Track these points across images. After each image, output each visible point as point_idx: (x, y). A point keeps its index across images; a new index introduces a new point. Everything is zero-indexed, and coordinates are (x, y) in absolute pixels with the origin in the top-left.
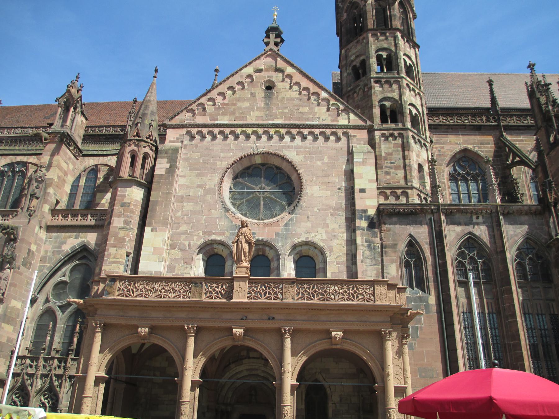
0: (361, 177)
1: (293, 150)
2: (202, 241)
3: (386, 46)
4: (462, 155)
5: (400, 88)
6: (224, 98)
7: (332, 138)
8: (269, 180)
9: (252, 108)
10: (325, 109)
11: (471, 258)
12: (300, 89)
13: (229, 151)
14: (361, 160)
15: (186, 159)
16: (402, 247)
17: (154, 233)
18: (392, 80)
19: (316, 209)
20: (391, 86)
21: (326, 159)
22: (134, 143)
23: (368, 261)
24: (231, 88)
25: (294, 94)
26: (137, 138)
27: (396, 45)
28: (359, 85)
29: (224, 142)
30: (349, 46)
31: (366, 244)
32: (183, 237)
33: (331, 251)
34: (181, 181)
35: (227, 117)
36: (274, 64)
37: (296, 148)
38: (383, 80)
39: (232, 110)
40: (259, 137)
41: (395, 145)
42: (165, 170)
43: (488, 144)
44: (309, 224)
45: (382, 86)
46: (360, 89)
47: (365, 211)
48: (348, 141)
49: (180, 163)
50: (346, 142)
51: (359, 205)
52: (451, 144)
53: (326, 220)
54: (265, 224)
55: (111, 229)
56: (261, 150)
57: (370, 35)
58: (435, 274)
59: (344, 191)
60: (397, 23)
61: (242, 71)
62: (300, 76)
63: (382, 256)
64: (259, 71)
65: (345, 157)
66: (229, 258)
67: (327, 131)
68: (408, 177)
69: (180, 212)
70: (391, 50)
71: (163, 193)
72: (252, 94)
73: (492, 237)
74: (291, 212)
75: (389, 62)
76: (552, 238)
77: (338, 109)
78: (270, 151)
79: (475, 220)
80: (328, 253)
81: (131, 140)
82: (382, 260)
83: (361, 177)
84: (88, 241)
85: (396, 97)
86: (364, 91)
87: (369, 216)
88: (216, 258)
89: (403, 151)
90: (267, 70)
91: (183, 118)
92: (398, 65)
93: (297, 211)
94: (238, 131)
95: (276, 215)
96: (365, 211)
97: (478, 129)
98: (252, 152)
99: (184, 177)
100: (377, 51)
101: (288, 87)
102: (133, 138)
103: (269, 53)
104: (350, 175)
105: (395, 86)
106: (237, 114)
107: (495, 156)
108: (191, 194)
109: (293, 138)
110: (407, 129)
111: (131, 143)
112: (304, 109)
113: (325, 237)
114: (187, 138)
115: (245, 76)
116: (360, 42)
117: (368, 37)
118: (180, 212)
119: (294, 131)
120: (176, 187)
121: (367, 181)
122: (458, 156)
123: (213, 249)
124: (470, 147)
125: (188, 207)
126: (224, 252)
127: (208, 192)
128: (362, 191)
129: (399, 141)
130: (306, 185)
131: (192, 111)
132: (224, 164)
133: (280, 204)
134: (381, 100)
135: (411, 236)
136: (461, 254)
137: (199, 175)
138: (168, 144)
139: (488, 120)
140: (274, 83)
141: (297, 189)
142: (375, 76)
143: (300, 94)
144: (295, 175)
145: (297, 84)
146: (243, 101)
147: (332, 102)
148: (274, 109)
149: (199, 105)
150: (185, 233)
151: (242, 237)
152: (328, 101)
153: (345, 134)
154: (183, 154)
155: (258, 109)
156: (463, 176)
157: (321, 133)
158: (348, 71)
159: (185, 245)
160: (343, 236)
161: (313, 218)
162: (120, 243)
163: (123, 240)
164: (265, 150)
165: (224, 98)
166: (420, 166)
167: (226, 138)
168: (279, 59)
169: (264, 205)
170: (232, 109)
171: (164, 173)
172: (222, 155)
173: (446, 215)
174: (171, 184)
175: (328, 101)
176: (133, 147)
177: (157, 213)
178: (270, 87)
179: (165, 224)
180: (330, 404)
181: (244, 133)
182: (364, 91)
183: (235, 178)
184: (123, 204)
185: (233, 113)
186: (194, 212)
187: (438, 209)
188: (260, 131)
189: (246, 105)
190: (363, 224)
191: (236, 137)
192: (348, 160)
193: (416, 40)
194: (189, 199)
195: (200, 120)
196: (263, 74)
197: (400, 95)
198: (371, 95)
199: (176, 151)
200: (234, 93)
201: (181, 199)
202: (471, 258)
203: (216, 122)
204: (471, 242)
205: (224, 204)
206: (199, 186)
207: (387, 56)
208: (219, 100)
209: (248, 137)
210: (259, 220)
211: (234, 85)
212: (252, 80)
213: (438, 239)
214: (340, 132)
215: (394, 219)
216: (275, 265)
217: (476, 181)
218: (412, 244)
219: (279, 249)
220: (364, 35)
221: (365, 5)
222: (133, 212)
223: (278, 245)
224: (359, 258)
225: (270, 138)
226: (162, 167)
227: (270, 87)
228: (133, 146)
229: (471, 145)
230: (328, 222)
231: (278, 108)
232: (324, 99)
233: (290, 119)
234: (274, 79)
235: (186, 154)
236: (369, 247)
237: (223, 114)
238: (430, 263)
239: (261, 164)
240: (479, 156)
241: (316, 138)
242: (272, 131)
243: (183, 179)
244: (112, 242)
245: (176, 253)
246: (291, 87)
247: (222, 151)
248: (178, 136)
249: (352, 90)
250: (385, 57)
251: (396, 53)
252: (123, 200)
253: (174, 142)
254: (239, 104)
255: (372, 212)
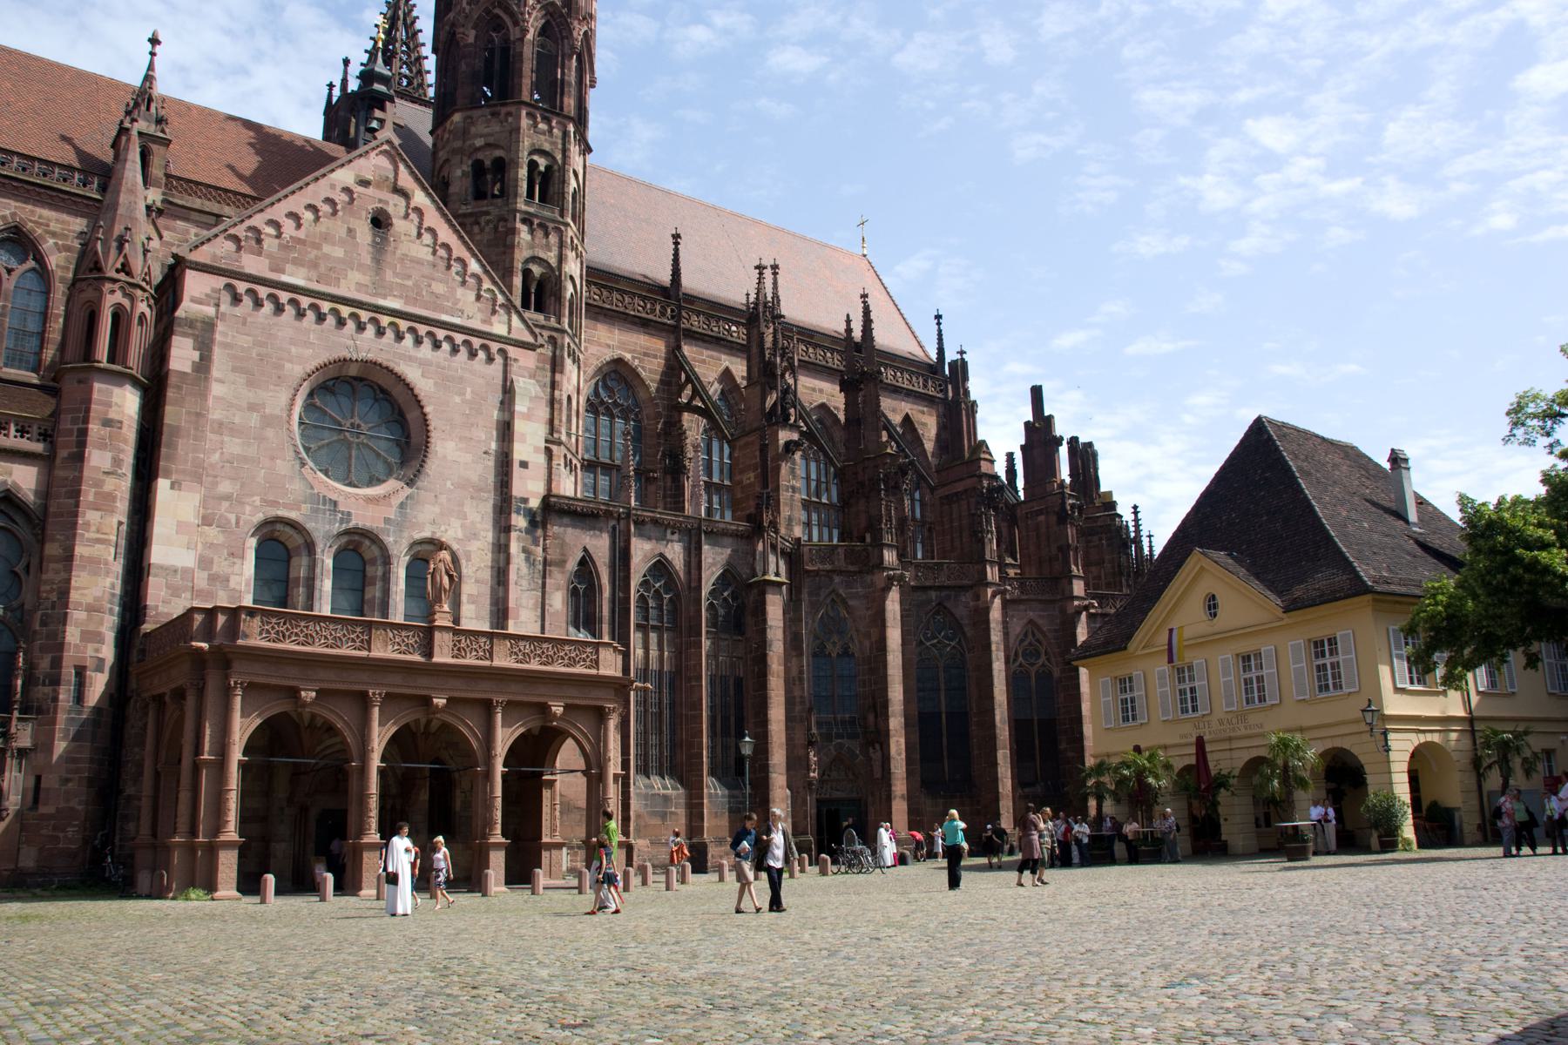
0: (523, 441)
1: (417, 365)
2: (259, 517)
3: (547, 147)
4: (613, 367)
5: (561, 245)
6: (299, 226)
7: (482, 355)
8: (369, 413)
9: (349, 263)
10: (472, 296)
11: (657, 591)
12: (435, 243)
13: (307, 344)
14: (525, 410)
15: (226, 346)
16: (572, 565)
17: (175, 493)
18: (551, 225)
19: (449, 484)
20: (547, 235)
21: (468, 396)
22: (122, 288)
23: (524, 583)
24: (312, 208)
25: (422, 251)
26: (122, 276)
27: (565, 151)
28: (487, 213)
29: (297, 324)
30: (476, 113)
31: (523, 556)
32: (226, 504)
33: (469, 560)
34: (216, 389)
35: (303, 271)
36: (391, 176)
37: (423, 363)
38: (536, 221)
39: (312, 256)
40: (361, 327)
41: (541, 358)
42: (190, 364)
43: (655, 357)
44: (437, 509)
45: (532, 232)
46: (488, 222)
47: (525, 501)
48: (505, 365)
49: (218, 353)
50: (501, 368)
51: (518, 489)
52: (600, 345)
53: (462, 505)
54: (370, 500)
55: (86, 473)
56: (362, 355)
57: (524, 113)
58: (613, 611)
59: (492, 458)
60: (570, 103)
61: (333, 175)
62: (437, 214)
63: (544, 577)
64: (365, 183)
65: (499, 396)
66: (304, 553)
67: (474, 342)
68: (556, 422)
69: (216, 456)
70: (554, 158)
71: (188, 413)
72: (350, 231)
73: (688, 564)
74: (410, 483)
75: (548, 184)
76: (755, 575)
77: (494, 300)
78: (380, 361)
79: (669, 536)
80: (463, 562)
81: (115, 281)
82: (544, 585)
83: (523, 441)
84: (14, 483)
85: (553, 262)
86: (496, 228)
87: (530, 510)
88: (280, 547)
89: (553, 371)
90: (378, 186)
91: (218, 253)
92: (563, 194)
93: (419, 484)
94: (326, 306)
95: (380, 481)
96: (525, 501)
97: (644, 325)
98: (348, 356)
99: (222, 382)
100: (530, 154)
101: (414, 232)
102: (116, 276)
103: (386, 147)
104: (506, 431)
105: (553, 239)
106: (322, 269)
107: (662, 382)
108: (237, 420)
109: (418, 341)
110: (563, 331)
111: (117, 286)
112: (439, 288)
113: (460, 535)
114: (226, 298)
115: (338, 189)
116: (502, 116)
117: (519, 118)
118: (216, 456)
119: (422, 329)
120: (210, 402)
121: (531, 449)
122: (605, 370)
123: (273, 531)
124: (628, 356)
125: (234, 446)
126: (296, 540)
127: (268, 421)
128: (524, 465)
129: (547, 351)
130: (435, 436)
131: (236, 239)
132: (296, 370)
133: (386, 461)
134: (527, 261)
135: (585, 550)
136: (645, 584)
137: (251, 384)
138: (186, 308)
139: (663, 314)
140: (388, 217)
141: (415, 440)
142: (524, 208)
143: (434, 253)
144: (417, 413)
145: (431, 230)
146: (333, 244)
147: (487, 285)
148: (389, 275)
149: (250, 228)
150: (228, 497)
151: (441, 566)
152: (479, 281)
153: (502, 352)
154: (221, 333)
155: (361, 267)
156: (607, 408)
157: (467, 343)
158: (465, 168)
159: (229, 521)
160: (488, 535)
161: (443, 499)
162: (105, 502)
163: (111, 497)
164: (371, 356)
165: (299, 226)
166: (569, 398)
167: (301, 314)
168: (402, 167)
169: (357, 458)
170: (313, 254)
171: (188, 369)
172: (293, 350)
173: (636, 523)
174: (204, 395)
175: (479, 281)
176: (118, 297)
177: (179, 452)
178: (380, 222)
179: (198, 478)
180: (458, 792)
181: (335, 312)
182: (496, 228)
183: (311, 395)
184: (107, 423)
185: (314, 265)
186: (245, 459)
187: (628, 515)
188: (365, 316)
189: (338, 252)
190: (519, 521)
191: (321, 318)
192: (502, 403)
193: (592, 134)
194: (234, 431)
195: (252, 264)
196: (370, 191)
197: (561, 259)
198: (512, 247)
199: (209, 325)
200: (317, 219)
201: (220, 427)
202: (657, 591)
203: (285, 278)
204: (661, 567)
205: (297, 453)
206: (252, 407)
207: (547, 168)
208: (288, 226)
209: (341, 323)
210: (350, 484)
211: (319, 204)
212: (352, 200)
213: (621, 558)
214: (495, 347)
215: (566, 520)
216: (380, 572)
217: (627, 420)
218: (586, 563)
219: (390, 547)
220: (512, 109)
221: (522, 40)
222: (125, 441)
223: (389, 540)
224: (513, 576)
225: (380, 332)
226: (182, 354)
227: (380, 222)
228: (119, 294)
229: (630, 351)
230: (467, 509)
231: (396, 274)
232: (474, 275)
233: (415, 302)
234: (390, 210)
235: (225, 334)
236: (527, 559)
237: (295, 262)
238: (607, 594)
239: (355, 378)
240: (638, 375)
241: (455, 350)
242: (385, 320)
243: (223, 387)
244: (91, 498)
245: (212, 533)
246: (419, 235)
247: (293, 342)
248: (208, 291)
249: (471, 214)
250: (542, 168)
251: (563, 170)
252: (107, 413)
253: (200, 302)
254: (326, 248)
255: (535, 503)
